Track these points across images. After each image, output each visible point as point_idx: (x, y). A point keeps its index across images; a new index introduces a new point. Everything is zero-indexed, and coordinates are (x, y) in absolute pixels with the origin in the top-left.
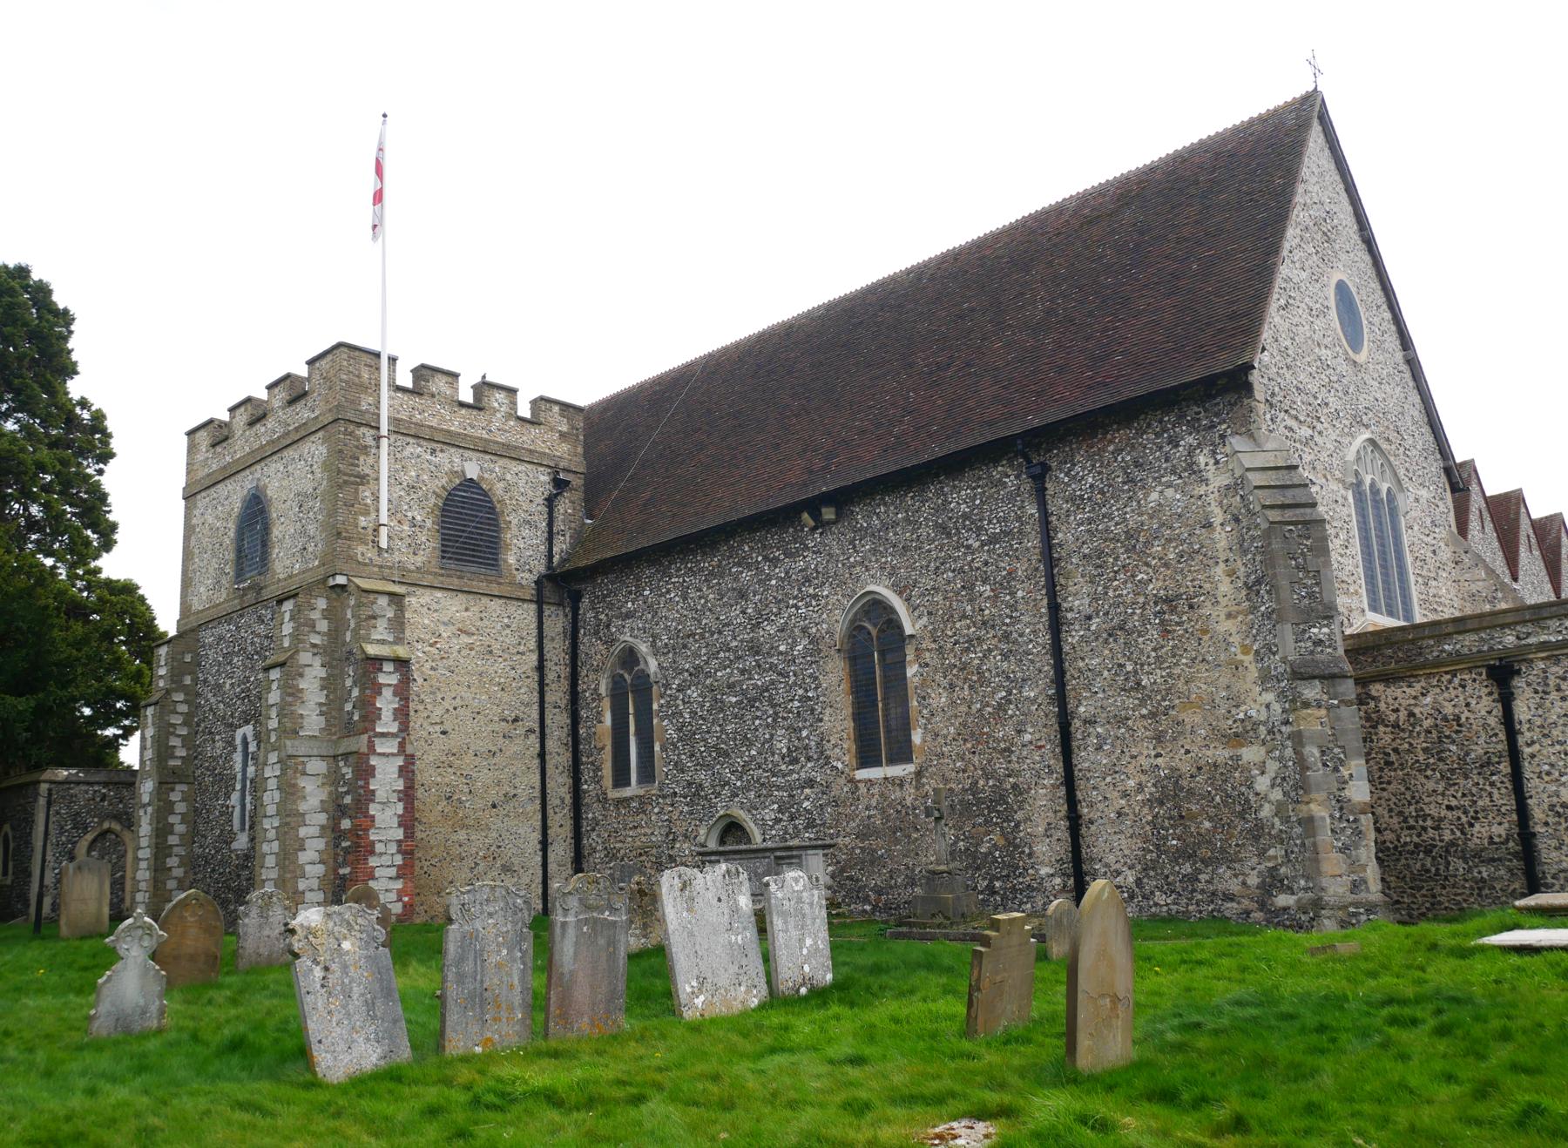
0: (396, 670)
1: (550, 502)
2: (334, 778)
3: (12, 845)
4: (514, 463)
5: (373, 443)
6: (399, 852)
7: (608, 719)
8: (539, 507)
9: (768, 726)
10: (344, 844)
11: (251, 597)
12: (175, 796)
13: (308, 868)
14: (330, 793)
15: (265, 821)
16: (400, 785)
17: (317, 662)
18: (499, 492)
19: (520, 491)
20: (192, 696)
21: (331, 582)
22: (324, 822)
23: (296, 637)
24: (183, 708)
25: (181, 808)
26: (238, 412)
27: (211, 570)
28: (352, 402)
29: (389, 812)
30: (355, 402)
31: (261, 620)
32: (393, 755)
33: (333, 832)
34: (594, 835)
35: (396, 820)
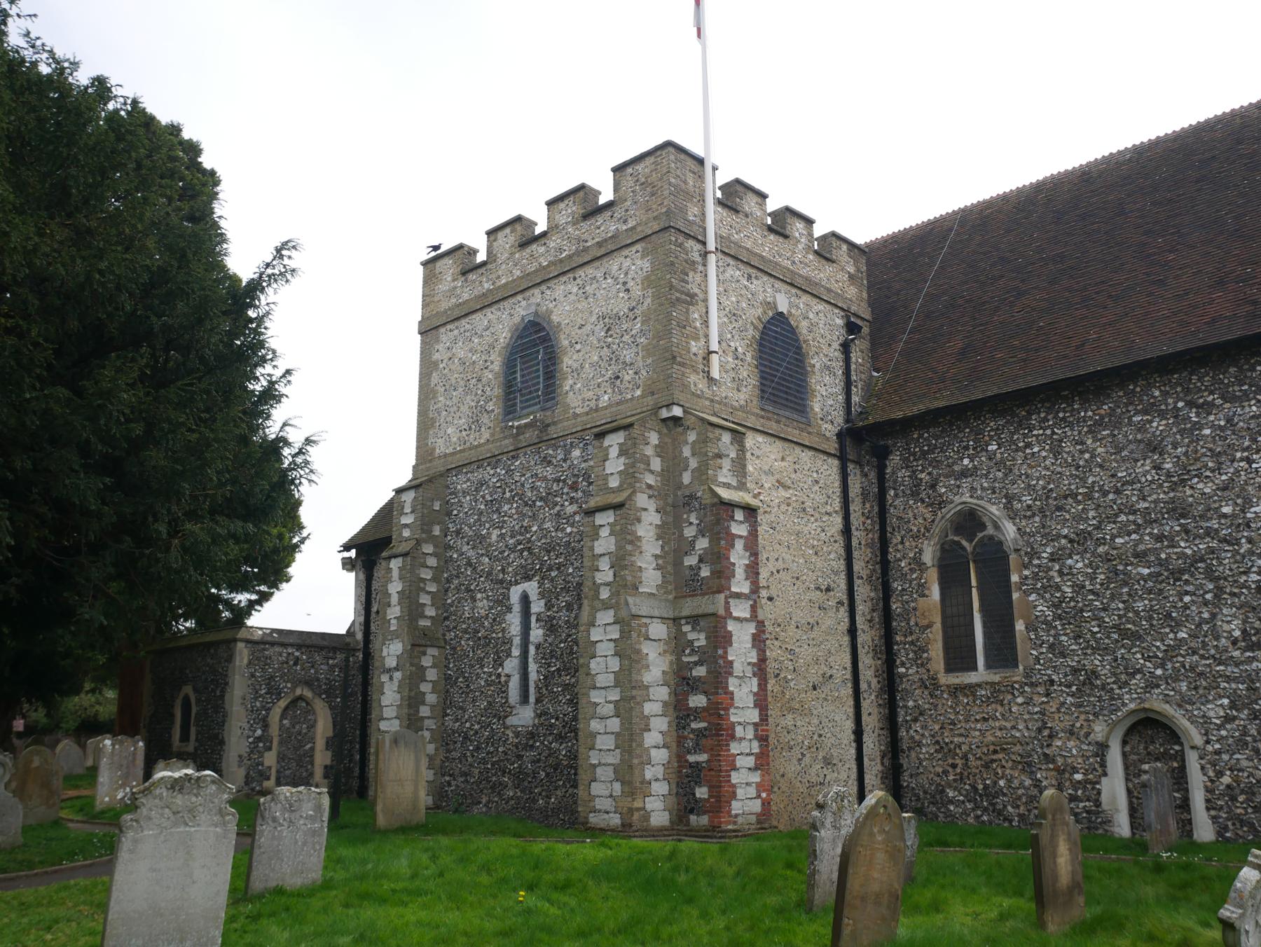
0: (746, 520)
1: (846, 347)
2: (678, 644)
3: (194, 710)
4: (815, 301)
5: (699, 259)
7: (935, 592)
8: (835, 352)
9: (1206, 603)
10: (693, 725)
11: (531, 436)
12: (426, 661)
13: (653, 752)
14: (671, 663)
15: (593, 693)
17: (652, 506)
18: (804, 331)
19: (821, 330)
20: (443, 549)
21: (664, 414)
22: (666, 698)
23: (629, 476)
24: (432, 562)
25: (432, 675)
26: (500, 235)
27: (464, 409)
28: (681, 210)
29: (745, 689)
30: (683, 211)
31: (547, 461)
32: (746, 620)
33: (681, 714)
34: (917, 727)
35: (751, 698)
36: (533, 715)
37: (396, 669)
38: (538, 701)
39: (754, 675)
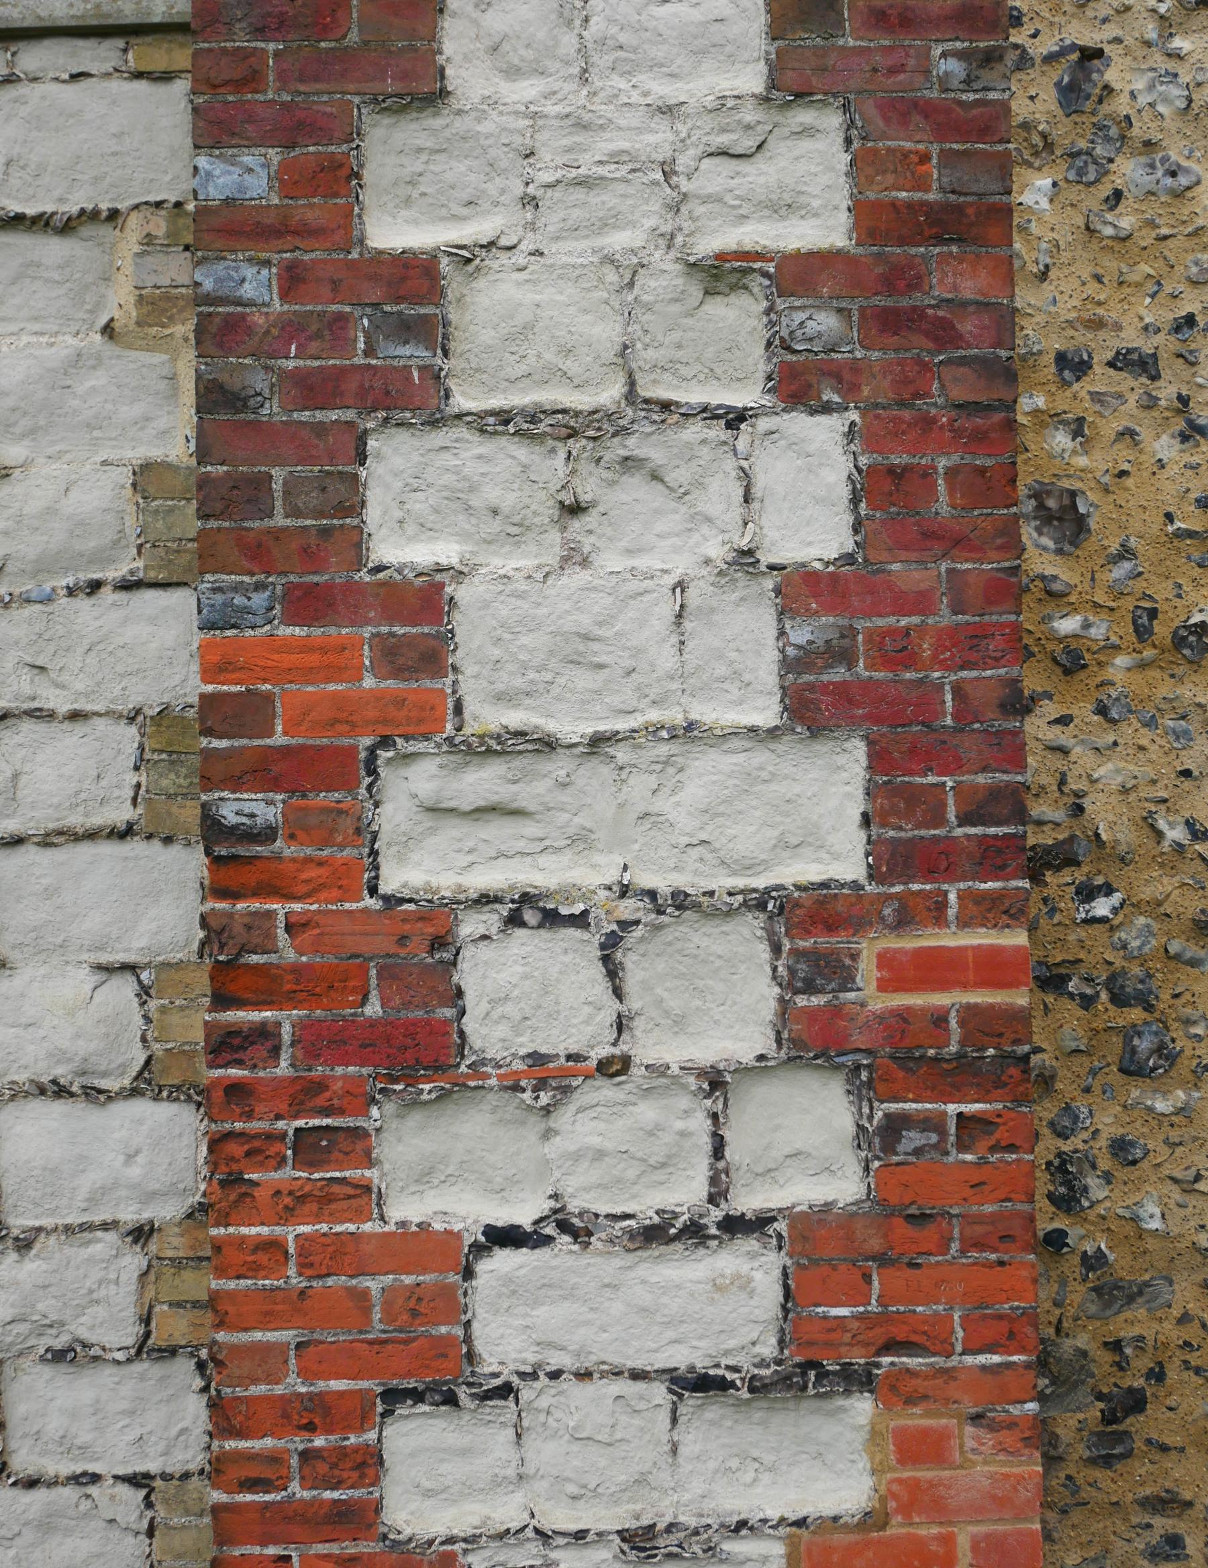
6: (809, 1041)
16: (805, 191)
29: (661, 537)
35: (748, 649)
39: (796, 386)
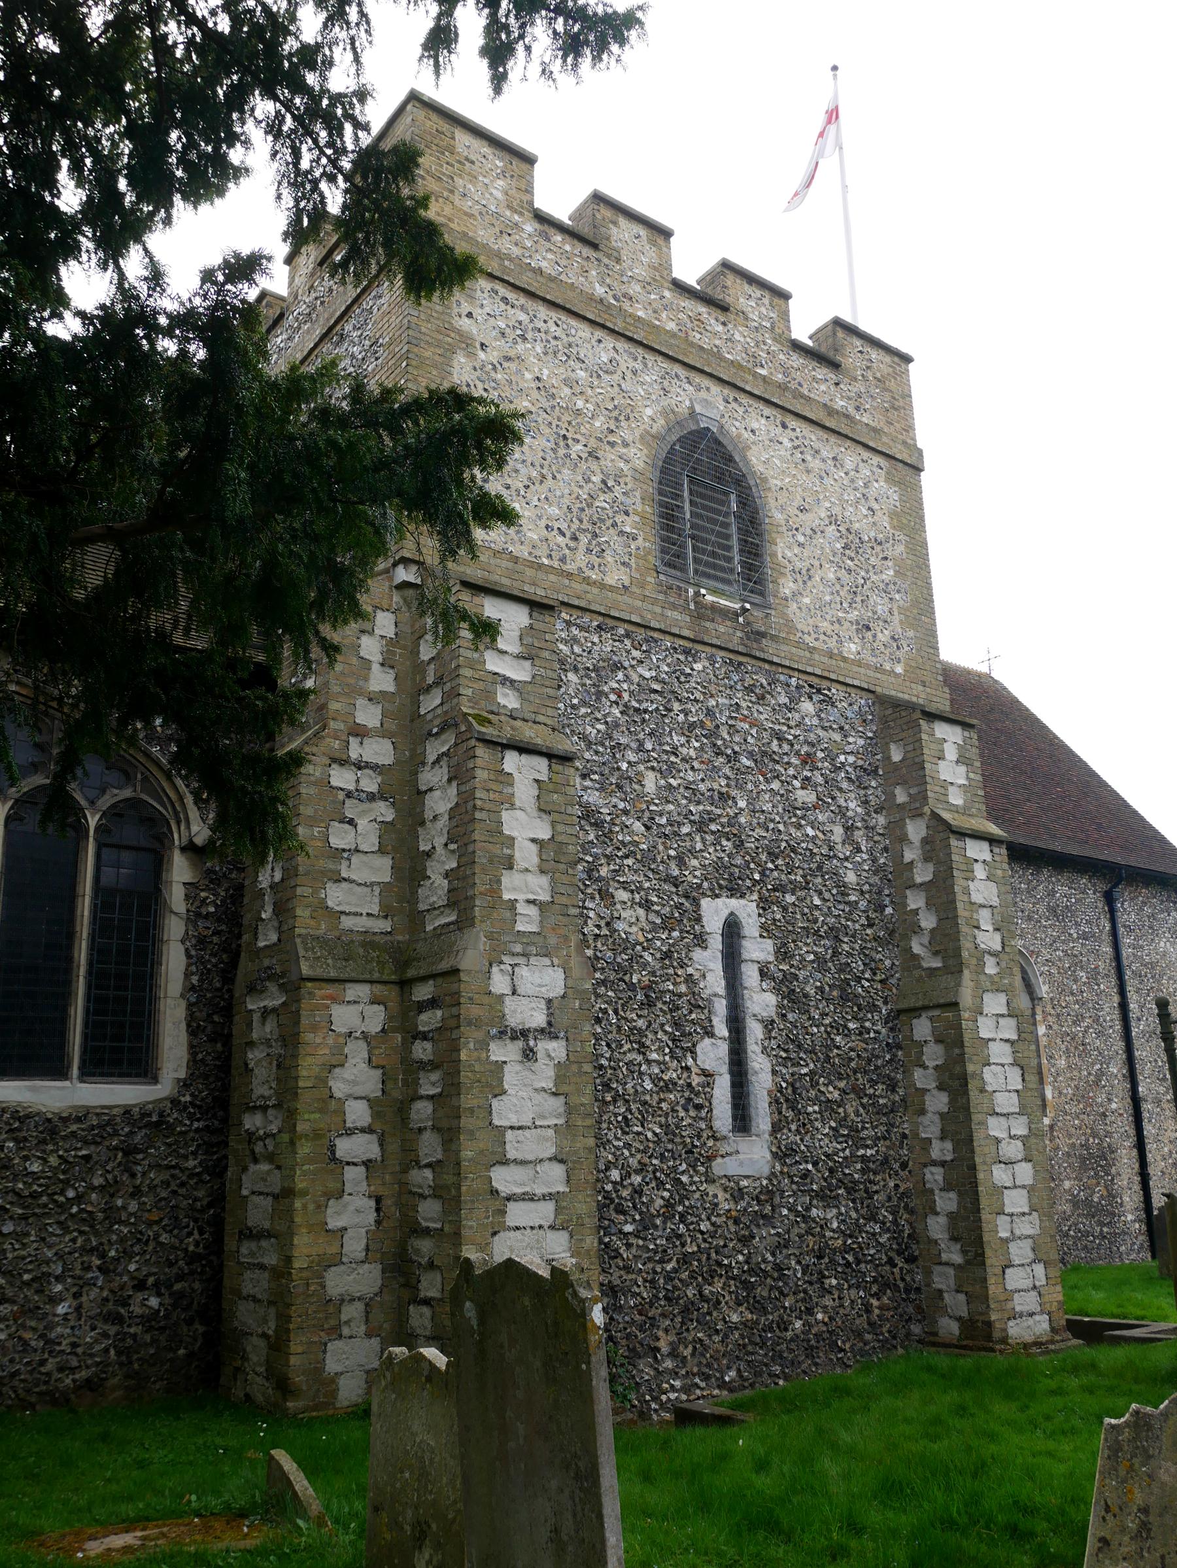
15: (992, 1121)
36: (768, 1156)
37: (548, 1032)
38: (776, 1128)
